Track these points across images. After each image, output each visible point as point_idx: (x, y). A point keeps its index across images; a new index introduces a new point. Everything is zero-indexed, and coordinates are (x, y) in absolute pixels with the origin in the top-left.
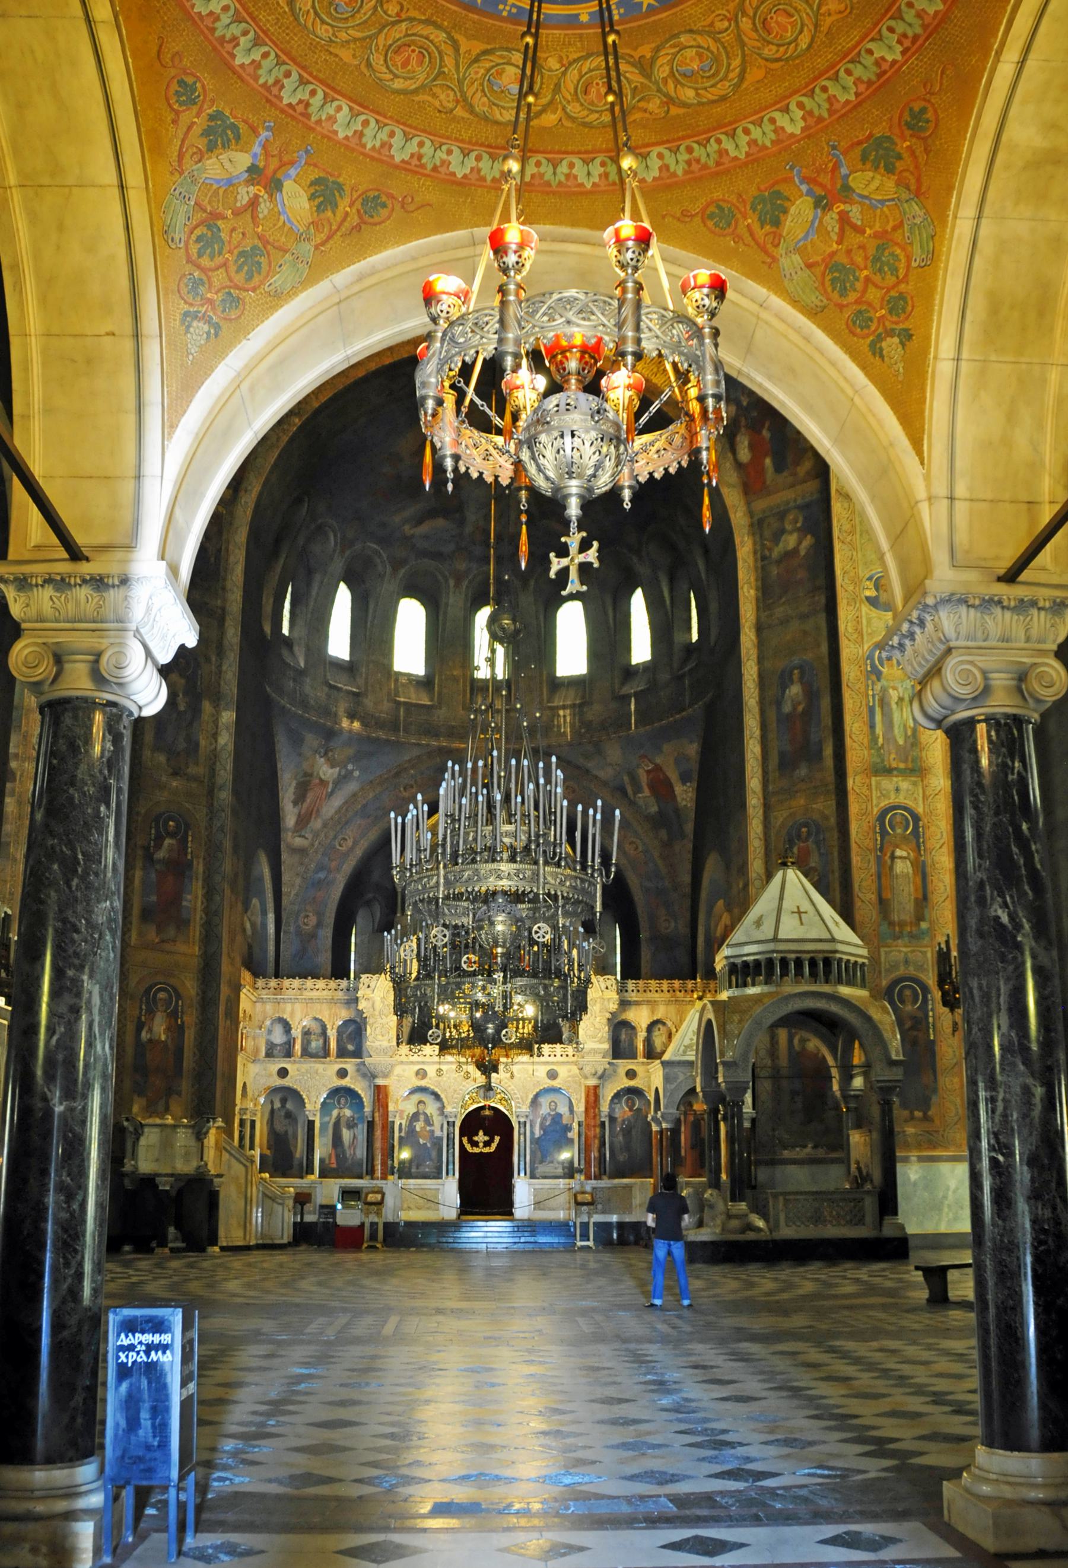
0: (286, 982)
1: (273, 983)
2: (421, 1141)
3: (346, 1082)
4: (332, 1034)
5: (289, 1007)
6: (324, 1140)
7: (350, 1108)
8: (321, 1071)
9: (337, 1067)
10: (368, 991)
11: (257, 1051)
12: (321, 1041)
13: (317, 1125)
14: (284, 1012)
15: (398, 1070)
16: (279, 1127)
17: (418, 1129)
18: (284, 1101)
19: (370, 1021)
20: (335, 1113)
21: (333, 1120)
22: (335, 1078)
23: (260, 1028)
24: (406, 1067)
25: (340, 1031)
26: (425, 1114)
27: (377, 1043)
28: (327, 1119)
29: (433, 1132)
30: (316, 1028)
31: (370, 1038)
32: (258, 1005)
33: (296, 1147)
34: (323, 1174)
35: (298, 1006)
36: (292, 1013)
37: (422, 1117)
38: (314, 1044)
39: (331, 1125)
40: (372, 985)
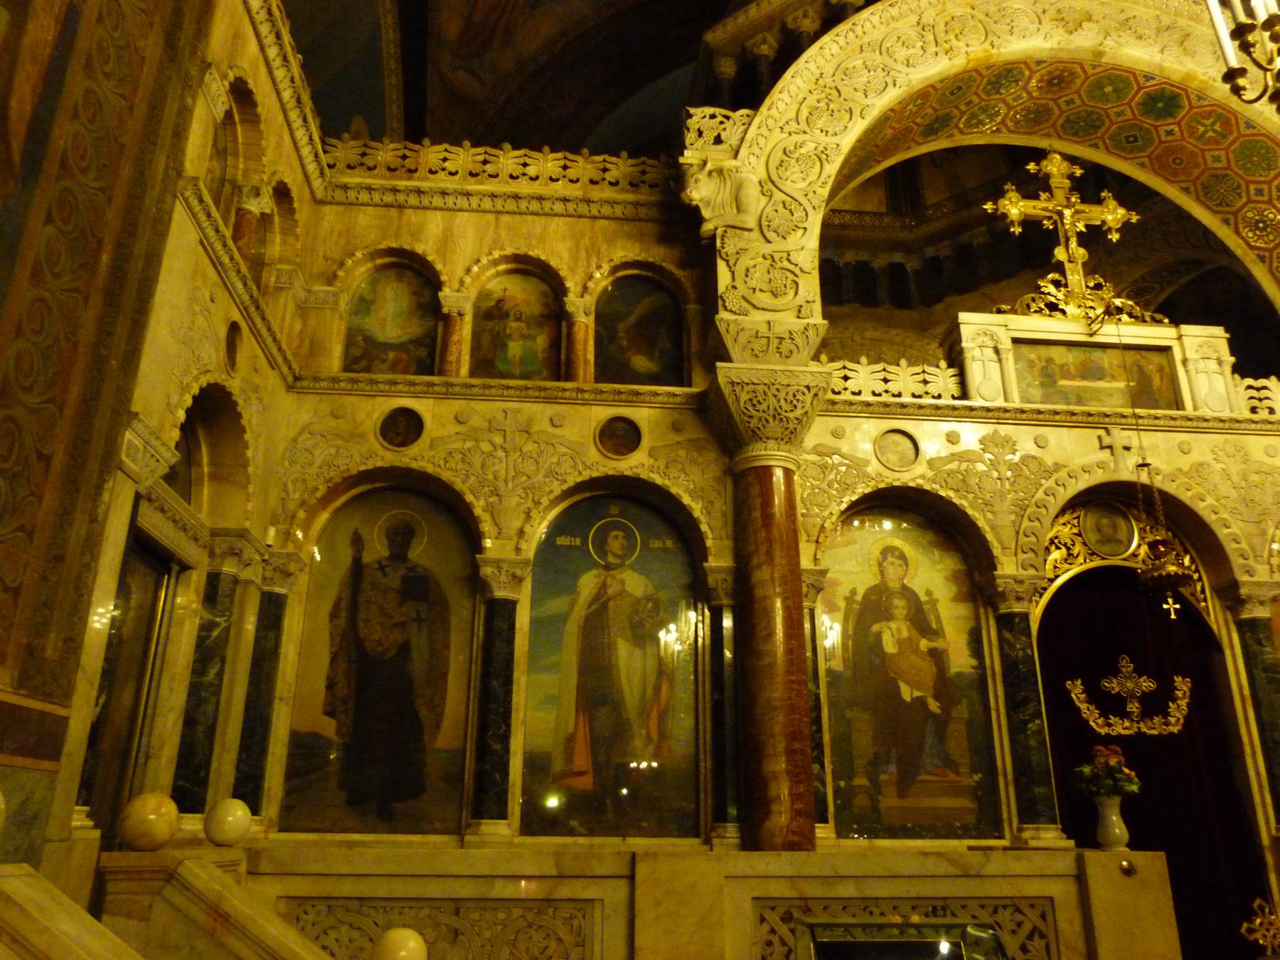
0: (432, 154)
1: (386, 153)
2: (907, 693)
3: (636, 463)
4: (581, 307)
5: (434, 223)
6: (548, 681)
7: (640, 568)
8: (543, 425)
9: (602, 413)
10: (718, 157)
11: (315, 348)
12: (541, 341)
13: (523, 618)
14: (416, 234)
15: (818, 432)
16: (374, 632)
17: (889, 646)
18: (401, 538)
19: (730, 246)
20: (588, 583)
21: (580, 611)
22: (593, 454)
23: (331, 279)
24: (847, 423)
25: (604, 318)
26: (907, 592)
27: (756, 319)
28: (556, 605)
29: (937, 656)
30: (521, 293)
31: (732, 300)
32: (327, 209)
33: (437, 708)
34: (536, 822)
35: (466, 224)
36: (447, 240)
37: (899, 604)
38: (515, 349)
39: (572, 630)
40: (731, 134)
